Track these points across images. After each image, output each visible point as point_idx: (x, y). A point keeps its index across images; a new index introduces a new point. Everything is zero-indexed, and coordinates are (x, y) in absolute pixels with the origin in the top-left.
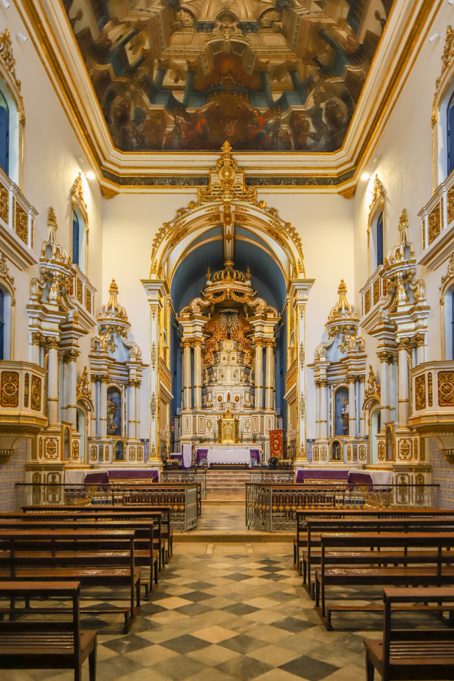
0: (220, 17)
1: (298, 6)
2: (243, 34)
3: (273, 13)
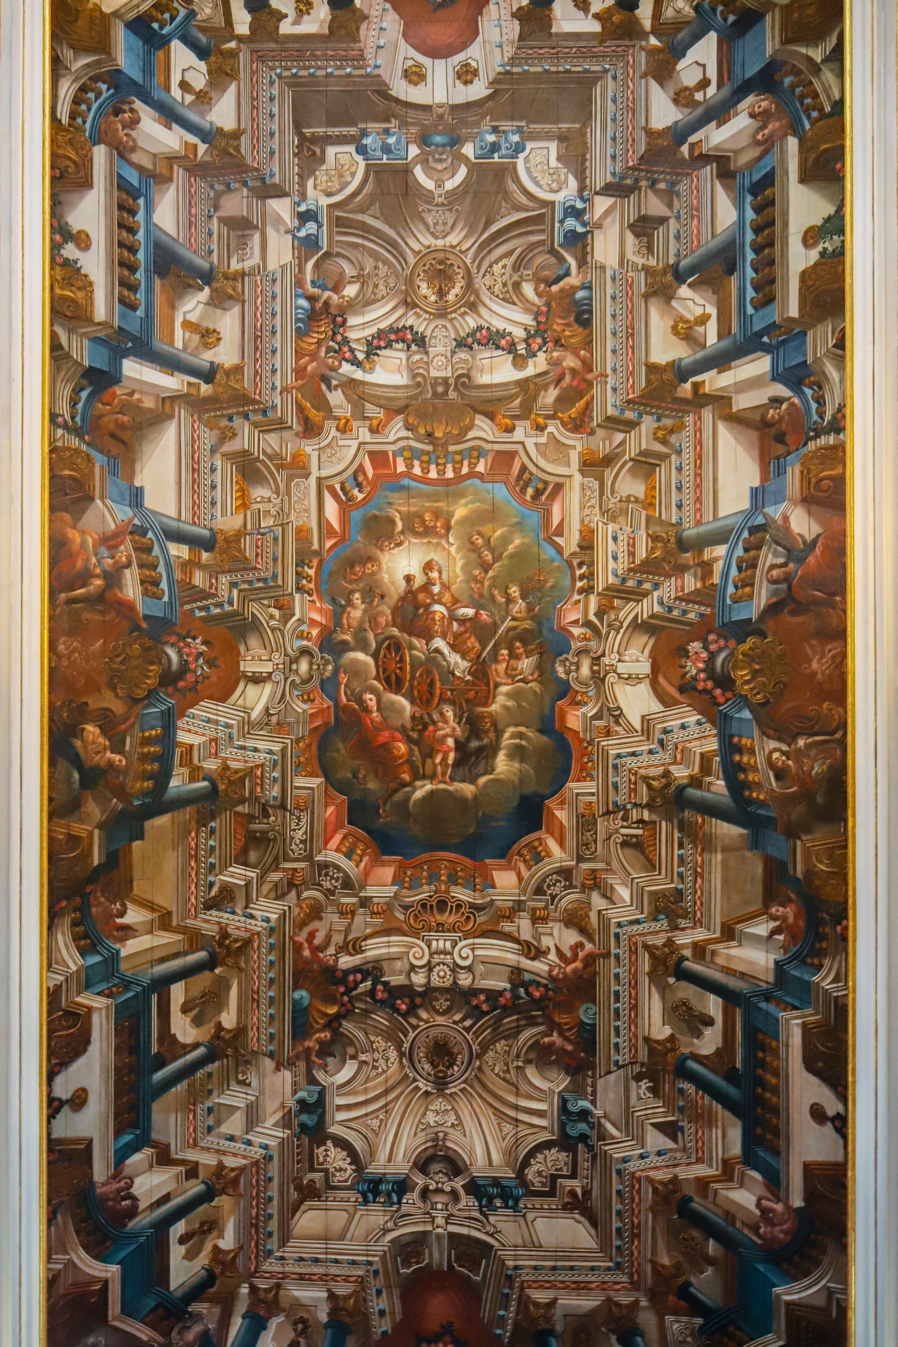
0: (423, 1165)
1: (613, 1138)
2: (481, 1212)
3: (553, 1154)
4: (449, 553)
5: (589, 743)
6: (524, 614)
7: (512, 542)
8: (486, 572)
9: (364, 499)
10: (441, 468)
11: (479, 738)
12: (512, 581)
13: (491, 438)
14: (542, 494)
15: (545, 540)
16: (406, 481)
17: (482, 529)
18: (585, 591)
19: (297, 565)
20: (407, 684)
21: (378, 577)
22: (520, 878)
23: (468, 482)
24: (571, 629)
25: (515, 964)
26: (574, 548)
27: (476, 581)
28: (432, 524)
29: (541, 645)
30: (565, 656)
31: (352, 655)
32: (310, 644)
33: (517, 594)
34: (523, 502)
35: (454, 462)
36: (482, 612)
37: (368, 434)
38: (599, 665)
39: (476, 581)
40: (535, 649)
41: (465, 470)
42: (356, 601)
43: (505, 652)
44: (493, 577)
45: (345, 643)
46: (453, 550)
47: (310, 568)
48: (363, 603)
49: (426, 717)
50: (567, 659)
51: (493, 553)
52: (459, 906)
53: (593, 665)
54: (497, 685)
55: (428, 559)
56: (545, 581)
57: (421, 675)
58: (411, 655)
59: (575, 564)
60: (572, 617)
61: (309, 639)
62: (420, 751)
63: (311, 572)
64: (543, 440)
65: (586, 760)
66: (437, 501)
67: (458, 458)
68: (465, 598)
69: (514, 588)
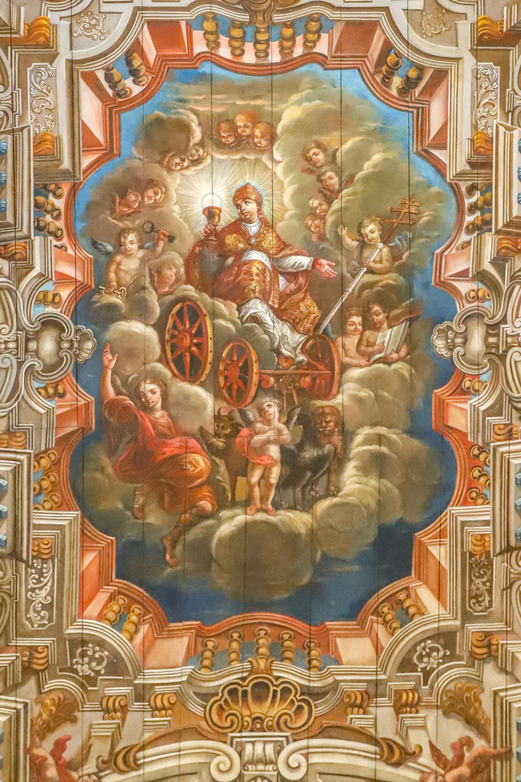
4: (273, 174)
5: (481, 450)
6: (386, 264)
7: (369, 158)
8: (330, 203)
12: (369, 216)
14: (416, 85)
15: (418, 154)
16: (207, 68)
17: (323, 139)
18: (479, 228)
19: (36, 193)
20: (208, 367)
22: (378, 648)
24: (456, 284)
25: (371, 775)
26: (462, 165)
28: (248, 131)
29: (411, 309)
30: (446, 323)
31: (123, 326)
32: (58, 311)
33: (376, 235)
34: (387, 99)
35: (282, 38)
36: (323, 261)
38: (497, 335)
39: (314, 215)
40: (402, 314)
41: (298, 51)
42: (129, 246)
43: (357, 319)
45: (112, 307)
46: (279, 170)
47: (59, 197)
50: (449, 328)
51: (339, 173)
52: (286, 691)
53: (488, 335)
55: (240, 184)
56: (418, 214)
57: (230, 355)
58: (213, 325)
59: (463, 189)
63: (60, 203)
65: (476, 474)
66: (256, 98)
67: (288, 32)
68: (297, 242)
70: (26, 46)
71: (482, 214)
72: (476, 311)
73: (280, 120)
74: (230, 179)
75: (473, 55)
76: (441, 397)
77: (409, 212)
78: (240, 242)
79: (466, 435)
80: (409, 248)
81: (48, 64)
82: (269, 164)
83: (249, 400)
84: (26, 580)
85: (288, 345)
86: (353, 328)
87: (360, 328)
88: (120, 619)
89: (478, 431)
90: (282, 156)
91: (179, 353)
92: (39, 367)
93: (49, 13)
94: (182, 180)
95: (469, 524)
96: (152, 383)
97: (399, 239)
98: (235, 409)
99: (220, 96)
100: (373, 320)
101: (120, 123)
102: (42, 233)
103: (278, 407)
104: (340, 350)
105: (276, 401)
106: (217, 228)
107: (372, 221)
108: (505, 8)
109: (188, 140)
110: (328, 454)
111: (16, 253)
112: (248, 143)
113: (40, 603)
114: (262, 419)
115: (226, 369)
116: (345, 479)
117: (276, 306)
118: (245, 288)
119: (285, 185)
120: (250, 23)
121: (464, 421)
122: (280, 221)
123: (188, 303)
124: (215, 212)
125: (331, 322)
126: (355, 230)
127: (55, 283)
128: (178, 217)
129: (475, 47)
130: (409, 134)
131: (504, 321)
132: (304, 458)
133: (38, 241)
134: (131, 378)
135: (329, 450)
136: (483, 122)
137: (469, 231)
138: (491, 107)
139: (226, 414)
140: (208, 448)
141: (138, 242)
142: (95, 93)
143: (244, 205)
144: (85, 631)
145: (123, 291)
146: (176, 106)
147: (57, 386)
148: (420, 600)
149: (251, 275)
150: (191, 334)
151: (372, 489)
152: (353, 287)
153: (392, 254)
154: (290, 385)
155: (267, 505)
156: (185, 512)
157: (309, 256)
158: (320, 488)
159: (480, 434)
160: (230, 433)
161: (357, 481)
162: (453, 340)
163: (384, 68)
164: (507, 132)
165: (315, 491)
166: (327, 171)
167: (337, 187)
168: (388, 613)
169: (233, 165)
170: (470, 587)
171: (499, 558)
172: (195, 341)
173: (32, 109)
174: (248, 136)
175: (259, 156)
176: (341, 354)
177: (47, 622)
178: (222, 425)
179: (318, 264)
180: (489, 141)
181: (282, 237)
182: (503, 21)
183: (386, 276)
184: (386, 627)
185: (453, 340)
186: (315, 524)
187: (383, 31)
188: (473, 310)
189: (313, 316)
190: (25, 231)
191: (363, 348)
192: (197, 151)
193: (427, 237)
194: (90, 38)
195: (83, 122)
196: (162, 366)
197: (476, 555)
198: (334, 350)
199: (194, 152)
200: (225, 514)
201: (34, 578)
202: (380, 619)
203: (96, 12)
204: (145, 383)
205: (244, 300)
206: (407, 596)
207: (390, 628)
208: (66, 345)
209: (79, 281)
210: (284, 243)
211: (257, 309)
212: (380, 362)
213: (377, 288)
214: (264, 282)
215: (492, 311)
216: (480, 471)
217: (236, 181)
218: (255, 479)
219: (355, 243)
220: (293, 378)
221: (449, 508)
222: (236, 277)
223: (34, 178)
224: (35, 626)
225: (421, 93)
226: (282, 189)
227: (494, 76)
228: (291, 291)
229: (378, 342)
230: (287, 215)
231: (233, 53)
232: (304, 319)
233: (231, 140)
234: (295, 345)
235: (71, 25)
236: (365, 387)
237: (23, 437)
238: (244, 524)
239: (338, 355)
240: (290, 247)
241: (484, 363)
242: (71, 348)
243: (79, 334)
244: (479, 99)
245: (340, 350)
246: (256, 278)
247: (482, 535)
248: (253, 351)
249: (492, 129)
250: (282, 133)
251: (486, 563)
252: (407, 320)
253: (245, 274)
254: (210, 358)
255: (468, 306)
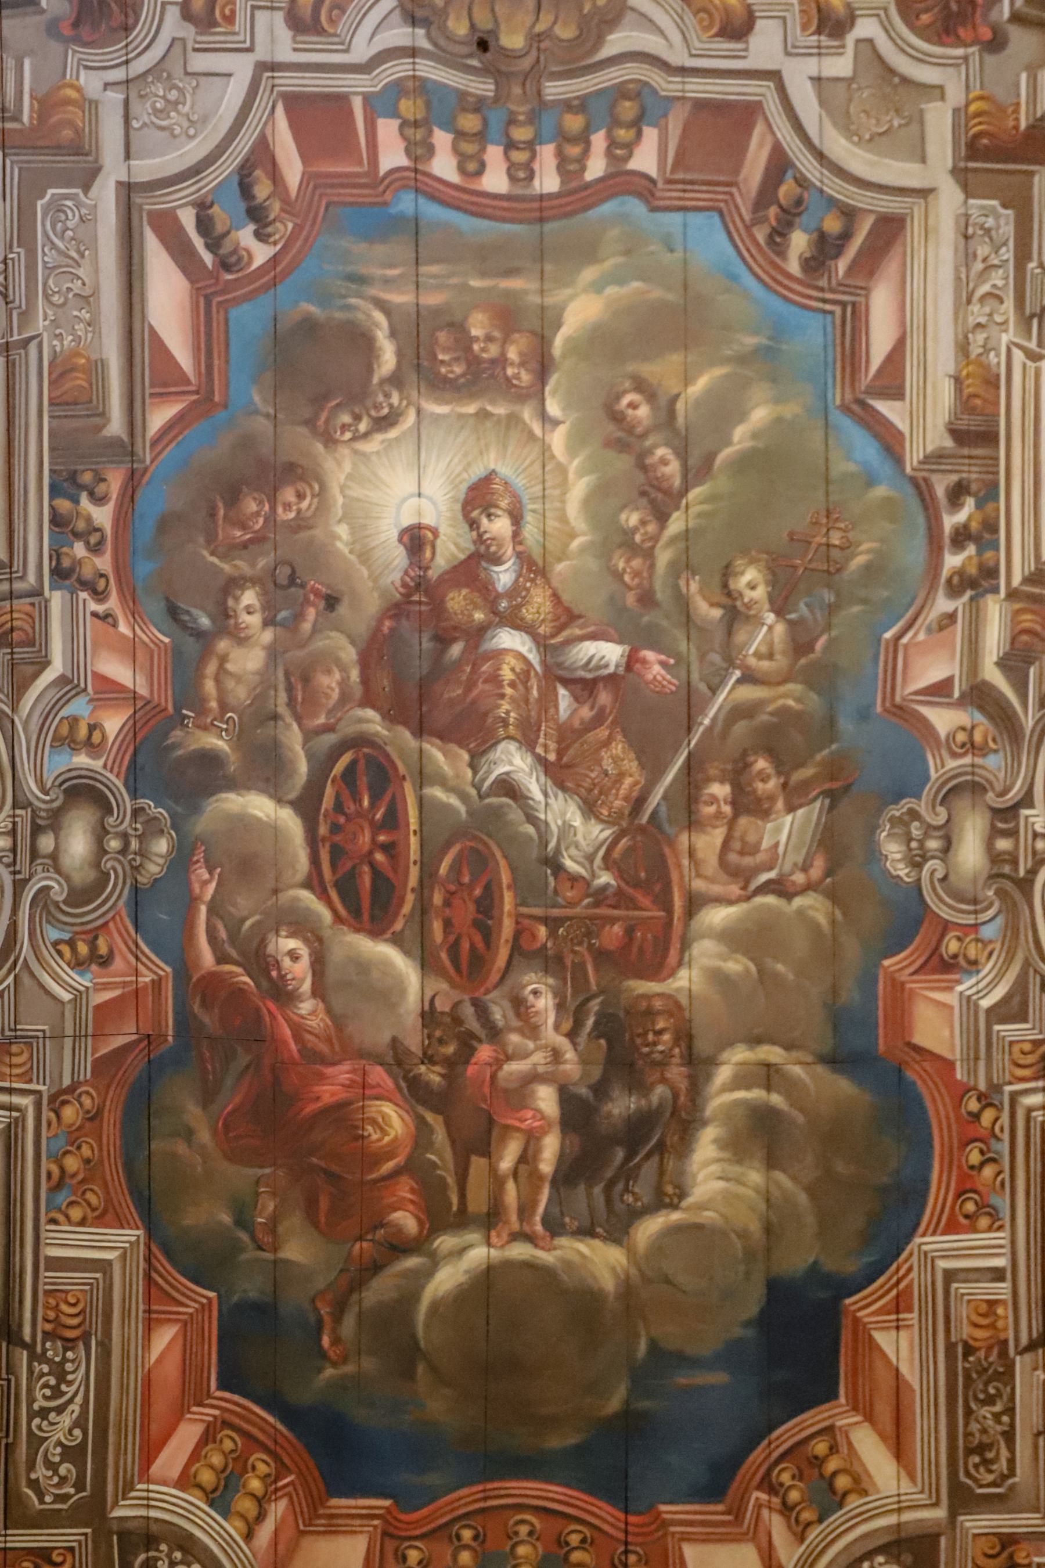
4: (545, 449)
5: (986, 1100)
7: (742, 416)
8: (662, 518)
9: (274, 260)
10: (520, 156)
11: (638, 1085)
12: (745, 552)
13: (678, 57)
14: (839, 253)
15: (845, 409)
16: (406, 203)
17: (648, 370)
18: (972, 583)
19: (55, 491)
20: (410, 898)
21: (318, 533)
23: (608, 208)
24: (926, 711)
27: (627, 543)
28: (494, 351)
29: (834, 769)
30: (907, 803)
31: (233, 802)
32: (97, 764)
33: (760, 593)
35: (563, 138)
36: (650, 655)
37: (284, 34)
38: (1013, 833)
40: (815, 778)
41: (596, 168)
42: (246, 619)
43: (720, 790)
44: (686, 535)
45: (209, 759)
46: (558, 440)
47: (99, 500)
48: (267, 623)
49: (468, 1011)
50: (914, 814)
51: (683, 455)
53: (995, 833)
54: (694, 904)
55: (477, 472)
56: (848, 547)
57: (456, 868)
59: (940, 491)
60: (935, 674)
61: (92, 747)
62: (448, 1125)
63: (103, 516)
64: (840, 66)
65: (975, 1158)
67: (574, 123)
69: (750, 574)
70: (35, 149)
71: (980, 552)
72: (969, 778)
73: (559, 326)
74: (456, 460)
75: (958, 181)
76: (897, 975)
77: (828, 545)
78: (476, 607)
79: (950, 1065)
80: (829, 627)
81: (78, 191)
82: (538, 431)
83: (494, 977)
84: (30, 1391)
85: (577, 847)
86: (711, 809)
87: (727, 809)
88: (226, 1486)
89: (977, 1058)
90: (564, 409)
91: (349, 865)
92: (59, 892)
93: (82, 72)
94: (355, 465)
95: (962, 1276)
96: (292, 935)
97: (807, 605)
98: (466, 997)
99: (434, 269)
100: (755, 791)
101: (227, 332)
102: (67, 582)
103: (555, 995)
104: (685, 862)
105: (551, 981)
106: (430, 573)
107: (752, 562)
108: (1024, 76)
109: (370, 370)
110: (660, 1105)
111: (12, 630)
112: (492, 376)
113: (59, 1443)
114: (520, 1024)
115: (447, 903)
116: (695, 1167)
117: (552, 757)
118: (486, 715)
119: (571, 476)
120: (496, 99)
121: (946, 1033)
122: (560, 560)
123: (366, 750)
124: (425, 536)
125: (665, 797)
126: (716, 580)
127: (91, 700)
128: (346, 551)
129: (962, 164)
130: (826, 363)
131: (1027, 800)
132: (609, 1114)
133: (57, 600)
134: (248, 923)
135: (661, 1098)
136: (980, 337)
137: (954, 590)
138: (994, 302)
139: (447, 1009)
140: (409, 1087)
141: (264, 609)
142: (176, 261)
143: (484, 521)
144: (153, 1514)
145: (231, 722)
146: (343, 292)
147: (96, 938)
148: (856, 1453)
149: (499, 684)
150: (372, 823)
151: (750, 1193)
152: (712, 713)
153: (793, 640)
154: (580, 944)
155: (531, 1224)
156: (361, 1238)
157: (620, 642)
158: (643, 1189)
159: (982, 1064)
160: (455, 1054)
161: (719, 1174)
162: (921, 843)
163: (773, 211)
164: (1029, 363)
165: (634, 1194)
166: (656, 446)
167: (677, 482)
168: (790, 1487)
169: (462, 428)
170: (966, 1424)
171: (1028, 1357)
172: (382, 838)
173: (47, 297)
174: (493, 362)
175: (516, 408)
176: (686, 871)
177: (72, 1491)
178: (438, 1033)
179: (637, 661)
180: (992, 382)
181: (565, 597)
182: (1018, 104)
183: (782, 689)
184: (787, 1518)
185: (921, 843)
186: (633, 1271)
187: (770, 126)
188: (966, 773)
189: (628, 781)
190: (32, 578)
191: (733, 857)
192: (387, 396)
193: (865, 601)
194: (165, 134)
195: (151, 328)
196: (312, 897)
197: (979, 1349)
198: (671, 861)
199: (381, 398)
200: (445, 1242)
201: (46, 1386)
202: (776, 1501)
203: (178, 71)
204: (278, 935)
205: (484, 742)
206: (831, 1448)
207: (797, 1521)
208: (114, 844)
209: (142, 697)
210: (568, 610)
211: (511, 763)
212: (767, 893)
213: (764, 718)
214: (527, 701)
215: (1002, 775)
216: (982, 1152)
217: (469, 465)
218: (506, 1164)
219: (717, 613)
220: (587, 928)
221: (918, 1240)
222: (469, 689)
223: (51, 457)
224: (48, 1499)
225: (850, 271)
226: (564, 485)
227: (1001, 231)
228: (582, 722)
229: (765, 844)
230: (575, 544)
231: (462, 170)
232: (610, 789)
233: (458, 369)
234: (591, 850)
235: (127, 103)
236: (736, 951)
237: (24, 1057)
238: (484, 1267)
239: (682, 877)
240: (581, 621)
241: (987, 898)
242: (124, 851)
243: (141, 819)
244: (971, 285)
245: (685, 862)
246: (508, 691)
247: (991, 1304)
248: (502, 863)
249: (998, 355)
250: (564, 356)
251: (1001, 1370)
252: (827, 793)
253: (486, 681)
254: (413, 880)
255: (952, 764)
